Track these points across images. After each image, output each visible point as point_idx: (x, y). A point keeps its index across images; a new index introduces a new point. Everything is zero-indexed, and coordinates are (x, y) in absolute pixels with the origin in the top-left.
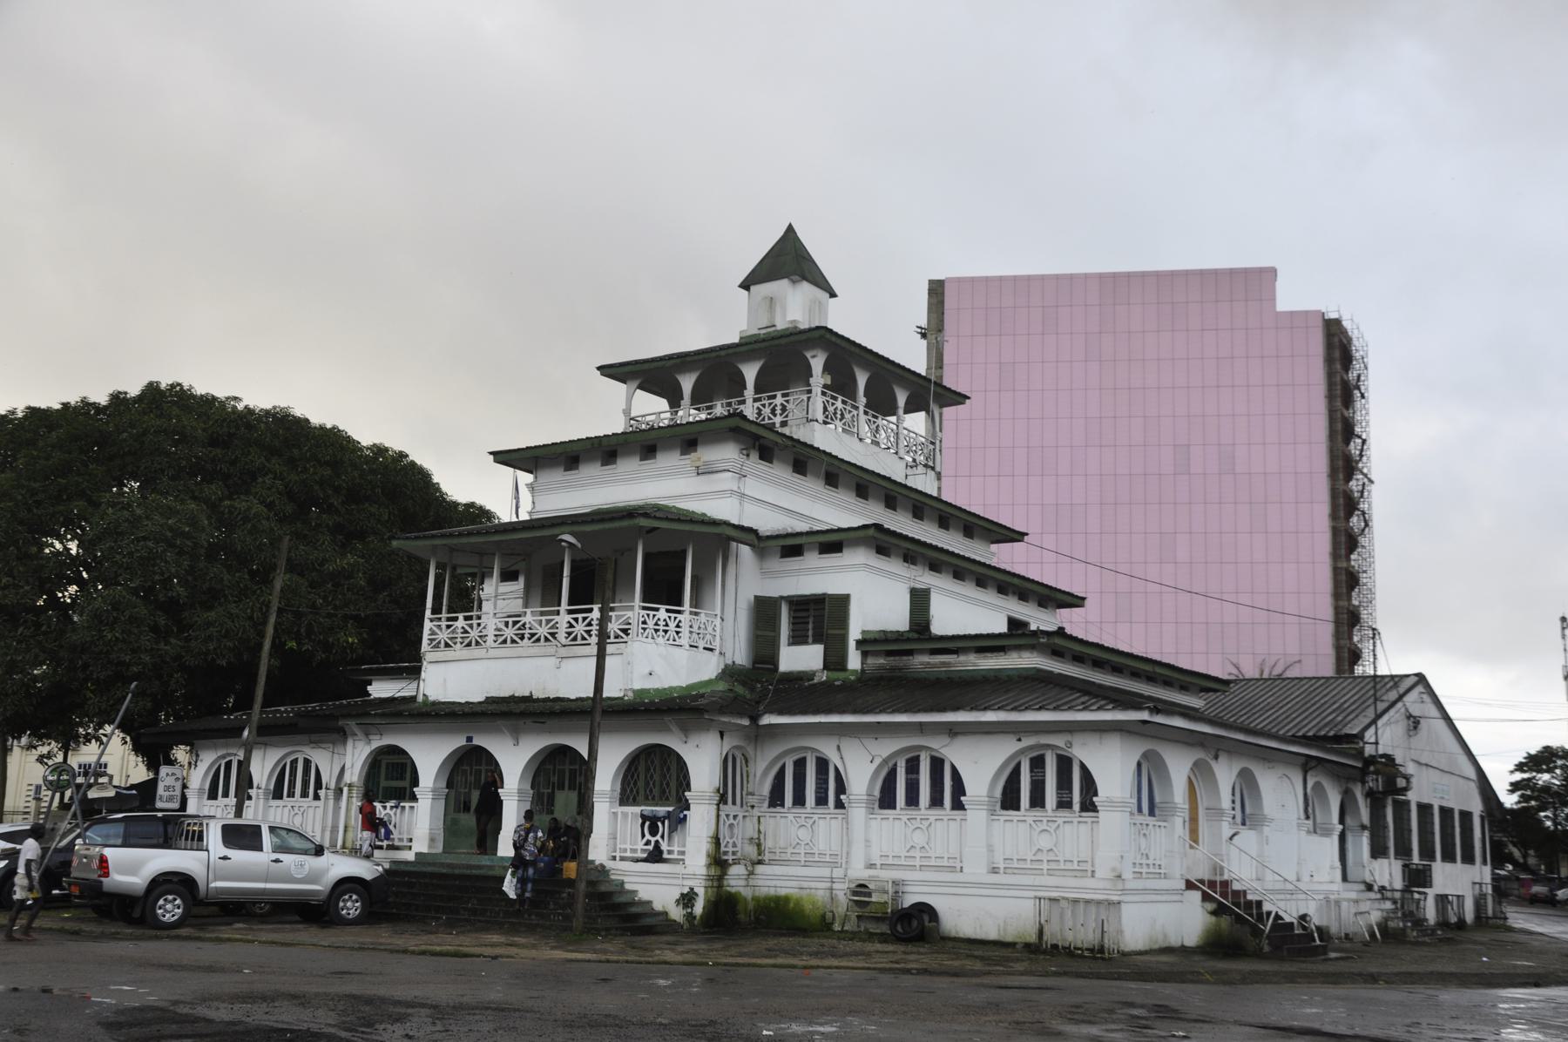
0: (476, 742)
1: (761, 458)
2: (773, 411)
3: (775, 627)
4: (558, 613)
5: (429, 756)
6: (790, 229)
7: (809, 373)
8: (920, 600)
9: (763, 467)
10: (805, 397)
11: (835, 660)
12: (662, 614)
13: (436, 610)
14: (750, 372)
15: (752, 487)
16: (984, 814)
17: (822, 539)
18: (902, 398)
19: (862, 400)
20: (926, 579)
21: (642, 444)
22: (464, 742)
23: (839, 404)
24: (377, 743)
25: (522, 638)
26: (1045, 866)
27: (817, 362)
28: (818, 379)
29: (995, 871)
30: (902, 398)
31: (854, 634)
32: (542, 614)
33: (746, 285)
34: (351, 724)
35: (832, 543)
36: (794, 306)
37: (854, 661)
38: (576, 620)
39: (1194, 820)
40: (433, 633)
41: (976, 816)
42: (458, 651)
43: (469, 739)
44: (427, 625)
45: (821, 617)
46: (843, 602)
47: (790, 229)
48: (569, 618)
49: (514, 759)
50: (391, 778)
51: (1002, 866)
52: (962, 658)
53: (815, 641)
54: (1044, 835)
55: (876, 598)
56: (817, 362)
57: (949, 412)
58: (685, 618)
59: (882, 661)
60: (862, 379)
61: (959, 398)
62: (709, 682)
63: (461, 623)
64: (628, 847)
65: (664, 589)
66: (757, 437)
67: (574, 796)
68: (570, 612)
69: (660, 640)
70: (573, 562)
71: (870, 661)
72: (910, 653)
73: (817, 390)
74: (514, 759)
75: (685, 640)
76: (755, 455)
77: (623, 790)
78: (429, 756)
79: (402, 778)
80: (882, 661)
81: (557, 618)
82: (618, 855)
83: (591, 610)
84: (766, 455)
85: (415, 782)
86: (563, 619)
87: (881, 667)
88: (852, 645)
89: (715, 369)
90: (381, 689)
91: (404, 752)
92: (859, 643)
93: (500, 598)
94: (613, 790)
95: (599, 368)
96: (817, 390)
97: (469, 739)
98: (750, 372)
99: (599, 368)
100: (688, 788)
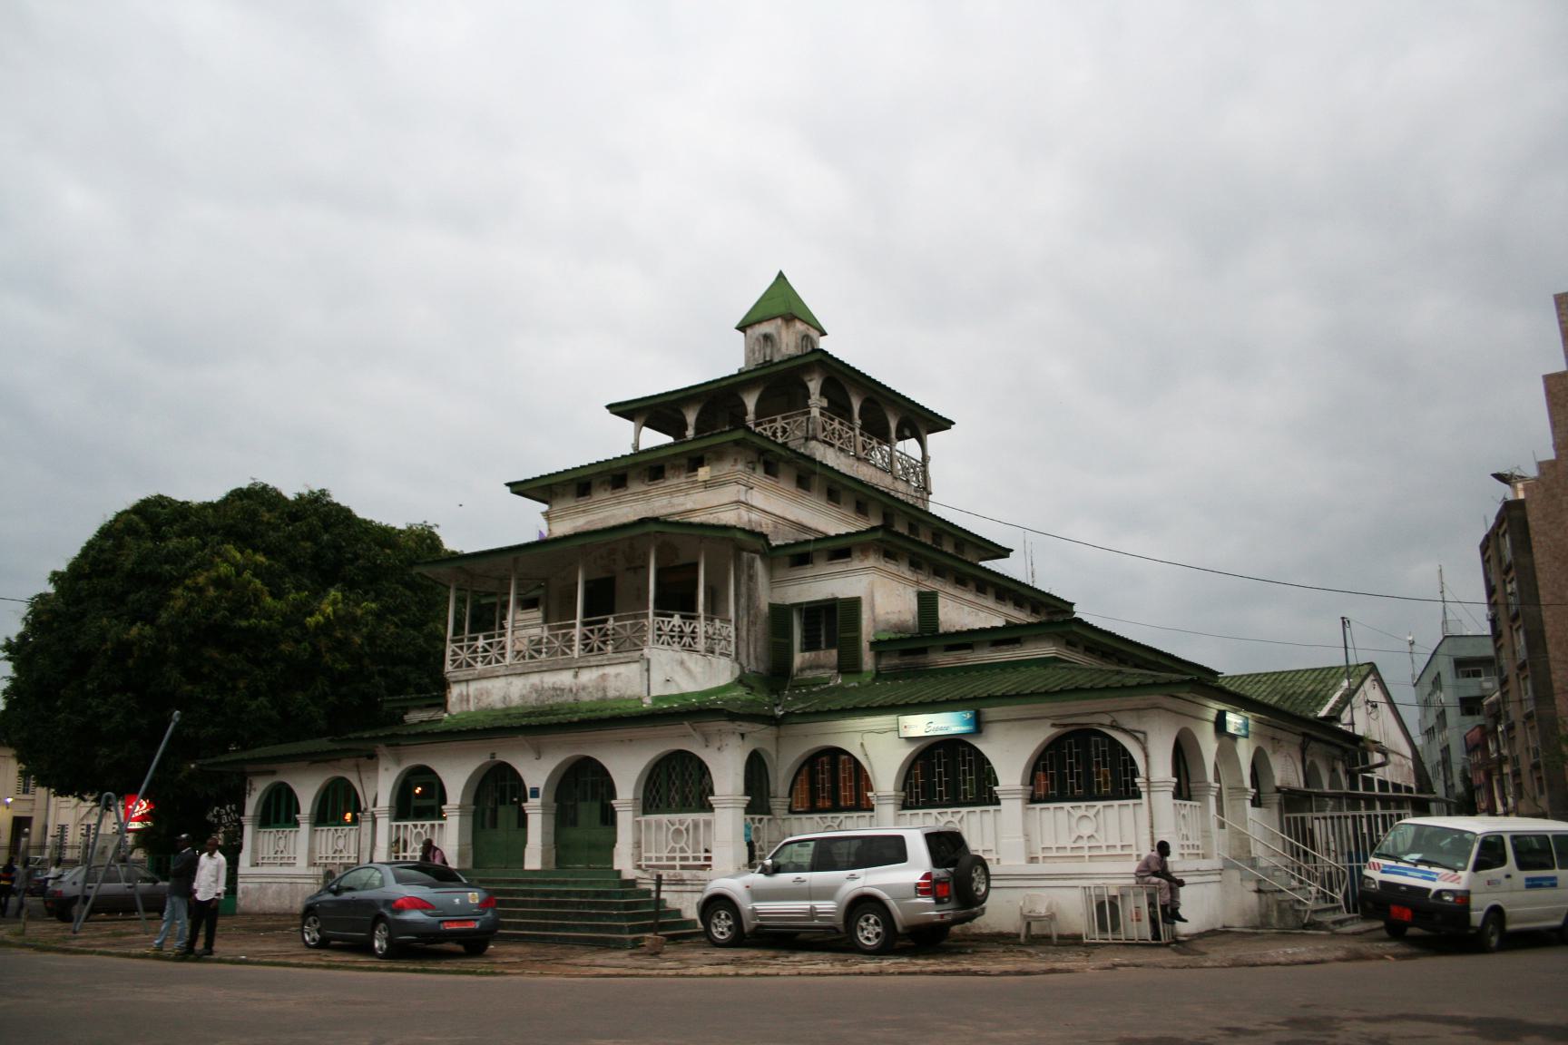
0: (500, 758)
1: (767, 472)
2: (774, 434)
3: (788, 634)
5: (456, 778)
6: (781, 276)
7: (807, 395)
8: (927, 604)
9: (769, 481)
10: (804, 418)
11: (849, 665)
12: (677, 620)
13: (459, 628)
14: (751, 402)
15: (757, 498)
16: (1019, 803)
17: (829, 544)
18: (893, 425)
19: (858, 422)
20: (931, 584)
21: (647, 468)
23: (836, 425)
24: (409, 763)
25: (539, 652)
26: (1086, 853)
27: (814, 386)
28: (817, 403)
29: (1033, 860)
30: (893, 425)
31: (867, 632)
32: (561, 627)
33: (742, 328)
34: (382, 749)
35: (840, 550)
36: (788, 342)
37: (868, 661)
39: (1219, 799)
40: (455, 654)
41: (1011, 807)
43: (493, 756)
44: (450, 648)
45: (833, 620)
46: (853, 605)
47: (781, 276)
48: (585, 630)
49: (536, 772)
50: (418, 799)
51: (1040, 855)
53: (830, 645)
54: (1085, 822)
55: (884, 596)
56: (814, 386)
57: (933, 439)
58: (701, 626)
59: (896, 661)
60: (856, 406)
61: (942, 424)
62: (726, 688)
63: (481, 642)
64: (653, 855)
65: (677, 598)
66: (762, 452)
67: (597, 805)
69: (676, 647)
70: (586, 583)
71: (884, 662)
72: (924, 651)
73: (815, 412)
74: (536, 772)
75: (701, 644)
76: (760, 471)
77: (645, 799)
78: (456, 778)
79: (432, 797)
80: (896, 661)
82: (643, 863)
83: (606, 621)
84: (771, 470)
85: (443, 800)
87: (896, 667)
88: (865, 645)
89: (716, 400)
90: (414, 717)
91: (432, 772)
92: (875, 645)
93: (523, 627)
94: (635, 799)
95: (609, 407)
96: (815, 412)
97: (493, 756)
98: (751, 402)
99: (609, 407)
100: (712, 792)
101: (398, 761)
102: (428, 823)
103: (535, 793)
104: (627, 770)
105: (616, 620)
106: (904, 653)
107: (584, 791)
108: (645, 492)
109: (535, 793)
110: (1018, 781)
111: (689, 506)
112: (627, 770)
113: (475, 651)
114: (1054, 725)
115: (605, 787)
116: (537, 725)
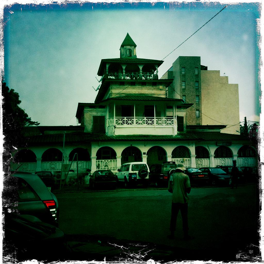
0: (133, 146)
4: (154, 118)
6: (128, 35)
22: (129, 146)
38: (159, 120)
42: (125, 125)
43: (131, 145)
48: (157, 119)
49: (144, 149)
52: (206, 130)
68: (156, 118)
72: (195, 128)
74: (144, 149)
78: (119, 150)
81: (153, 119)
86: (155, 120)
97: (131, 145)
101: (99, 146)
102: (109, 160)
103: (144, 153)
104: (169, 150)
105: (165, 118)
106: (190, 128)
107: (157, 154)
108: (142, 88)
109: (144, 153)
110: (237, 154)
111: (153, 93)
112: (169, 150)
113: (124, 121)
114: (243, 145)
115: (164, 153)
116: (145, 139)
